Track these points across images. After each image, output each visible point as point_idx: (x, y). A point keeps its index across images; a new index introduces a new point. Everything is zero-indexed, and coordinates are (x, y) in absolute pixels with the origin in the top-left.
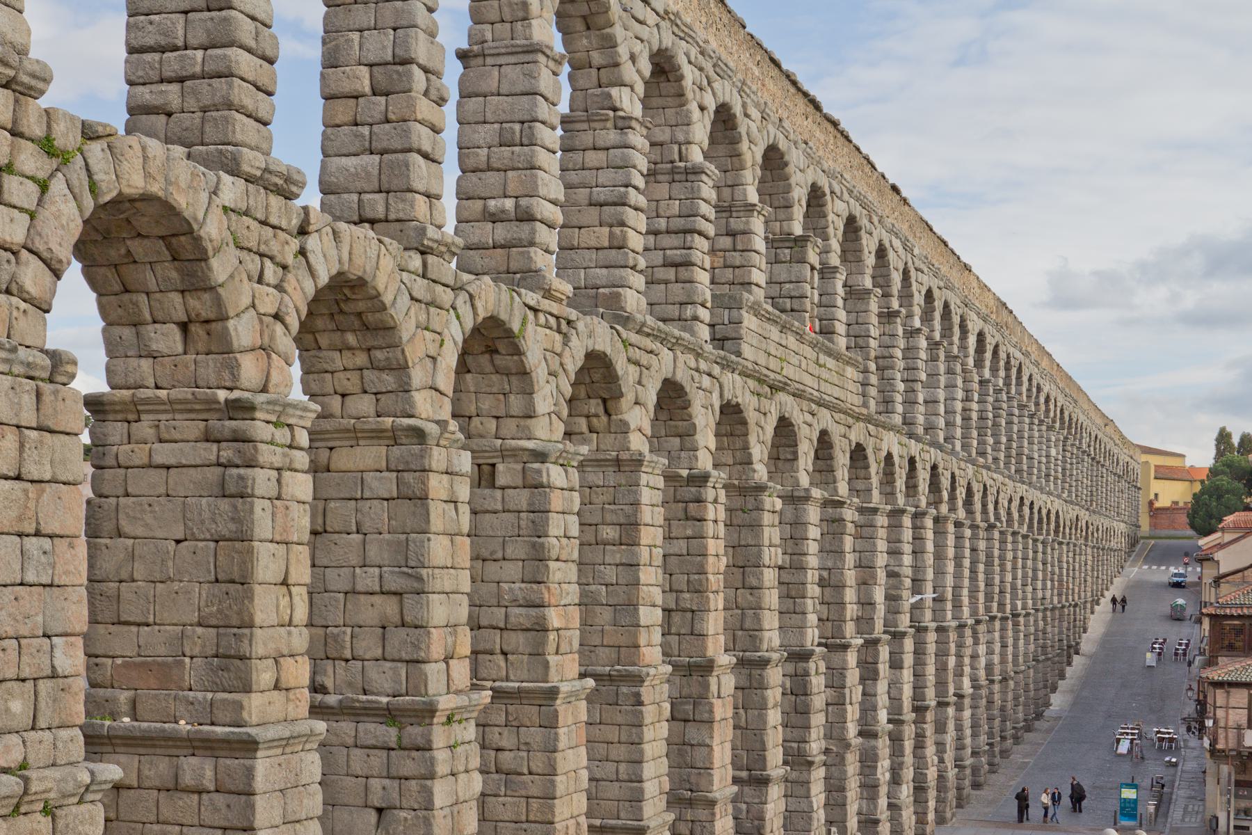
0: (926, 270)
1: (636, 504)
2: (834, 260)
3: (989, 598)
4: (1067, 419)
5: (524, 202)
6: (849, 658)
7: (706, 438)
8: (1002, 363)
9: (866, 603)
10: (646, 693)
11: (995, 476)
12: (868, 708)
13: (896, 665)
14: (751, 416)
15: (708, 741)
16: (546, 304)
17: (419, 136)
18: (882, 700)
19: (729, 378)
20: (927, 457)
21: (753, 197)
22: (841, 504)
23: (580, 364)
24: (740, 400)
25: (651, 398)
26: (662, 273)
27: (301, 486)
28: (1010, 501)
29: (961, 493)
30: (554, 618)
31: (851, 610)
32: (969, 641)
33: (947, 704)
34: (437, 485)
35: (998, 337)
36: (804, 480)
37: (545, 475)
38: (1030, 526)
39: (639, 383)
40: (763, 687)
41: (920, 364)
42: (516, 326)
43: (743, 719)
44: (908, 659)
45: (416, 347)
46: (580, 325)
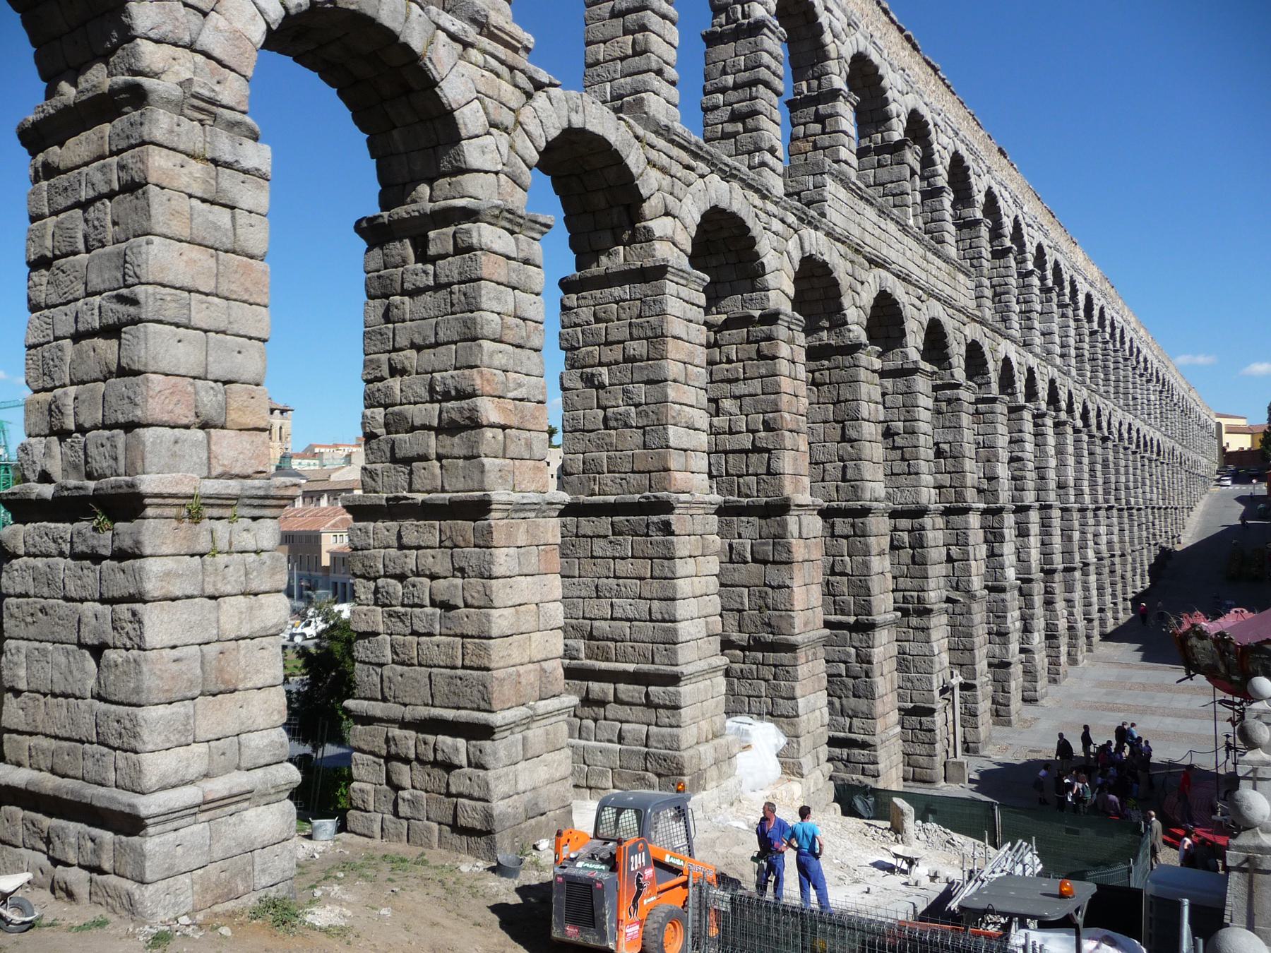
1: (663, 313)
2: (942, 181)
3: (1107, 492)
13: (1023, 533)
15: (788, 582)
16: (485, 42)
19: (807, 232)
20: (1045, 371)
22: (957, 386)
23: (554, 133)
24: (826, 258)
25: (692, 212)
26: (730, 128)
28: (1121, 424)
29: (1078, 409)
32: (1091, 521)
33: (1074, 569)
35: (1103, 302)
36: (914, 355)
37: (475, 234)
38: (1138, 446)
42: (417, 44)
44: (1034, 528)
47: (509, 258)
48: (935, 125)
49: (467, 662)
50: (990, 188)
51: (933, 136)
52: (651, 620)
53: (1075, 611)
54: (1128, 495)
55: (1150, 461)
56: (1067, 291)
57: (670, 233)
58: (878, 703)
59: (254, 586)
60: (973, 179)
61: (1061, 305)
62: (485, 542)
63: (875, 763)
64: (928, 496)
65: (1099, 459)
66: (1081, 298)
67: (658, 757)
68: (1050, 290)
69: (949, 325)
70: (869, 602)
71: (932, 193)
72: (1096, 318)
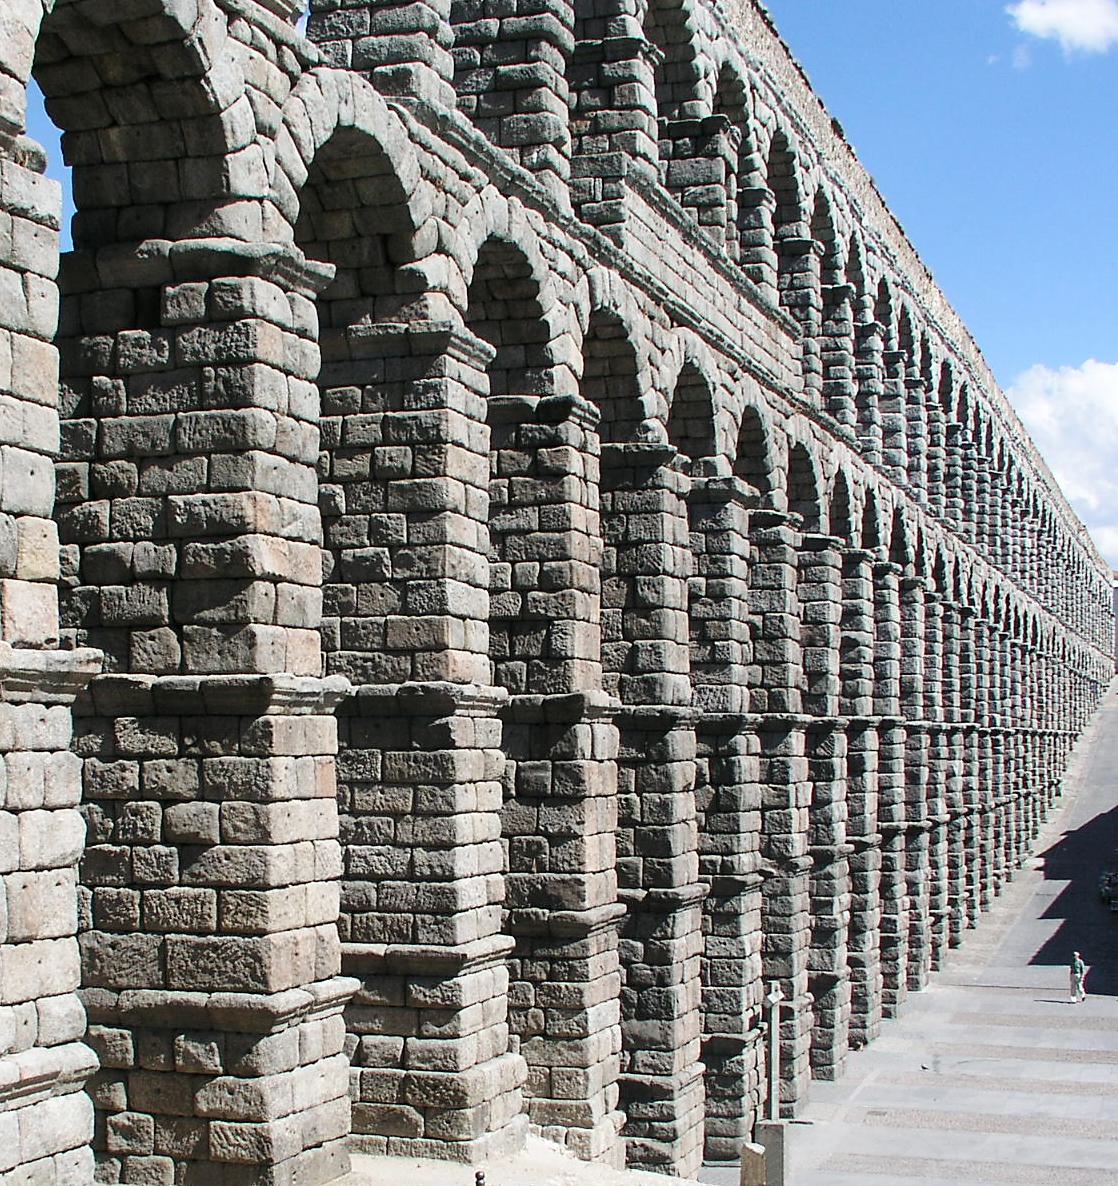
0: (878, 252)
1: (440, 404)
2: (759, 180)
4: (1040, 508)
6: (793, 741)
9: (815, 675)
10: (460, 725)
11: (968, 550)
15: (576, 828)
18: (839, 810)
19: (599, 271)
22: (778, 520)
24: (619, 312)
30: (265, 555)
31: (795, 673)
35: (965, 377)
36: (725, 470)
37: (246, 293)
38: (1007, 627)
43: (637, 810)
47: (284, 328)
48: (753, 87)
49: (228, 922)
50: (820, 187)
51: (749, 105)
52: (412, 880)
55: (1024, 649)
56: (917, 358)
57: (445, 282)
58: (677, 1023)
59: (53, 800)
60: (799, 172)
61: (911, 384)
63: (671, 1118)
64: (739, 699)
65: (957, 647)
66: (936, 369)
68: (896, 357)
69: (769, 418)
70: (669, 865)
71: (749, 201)
72: (954, 405)
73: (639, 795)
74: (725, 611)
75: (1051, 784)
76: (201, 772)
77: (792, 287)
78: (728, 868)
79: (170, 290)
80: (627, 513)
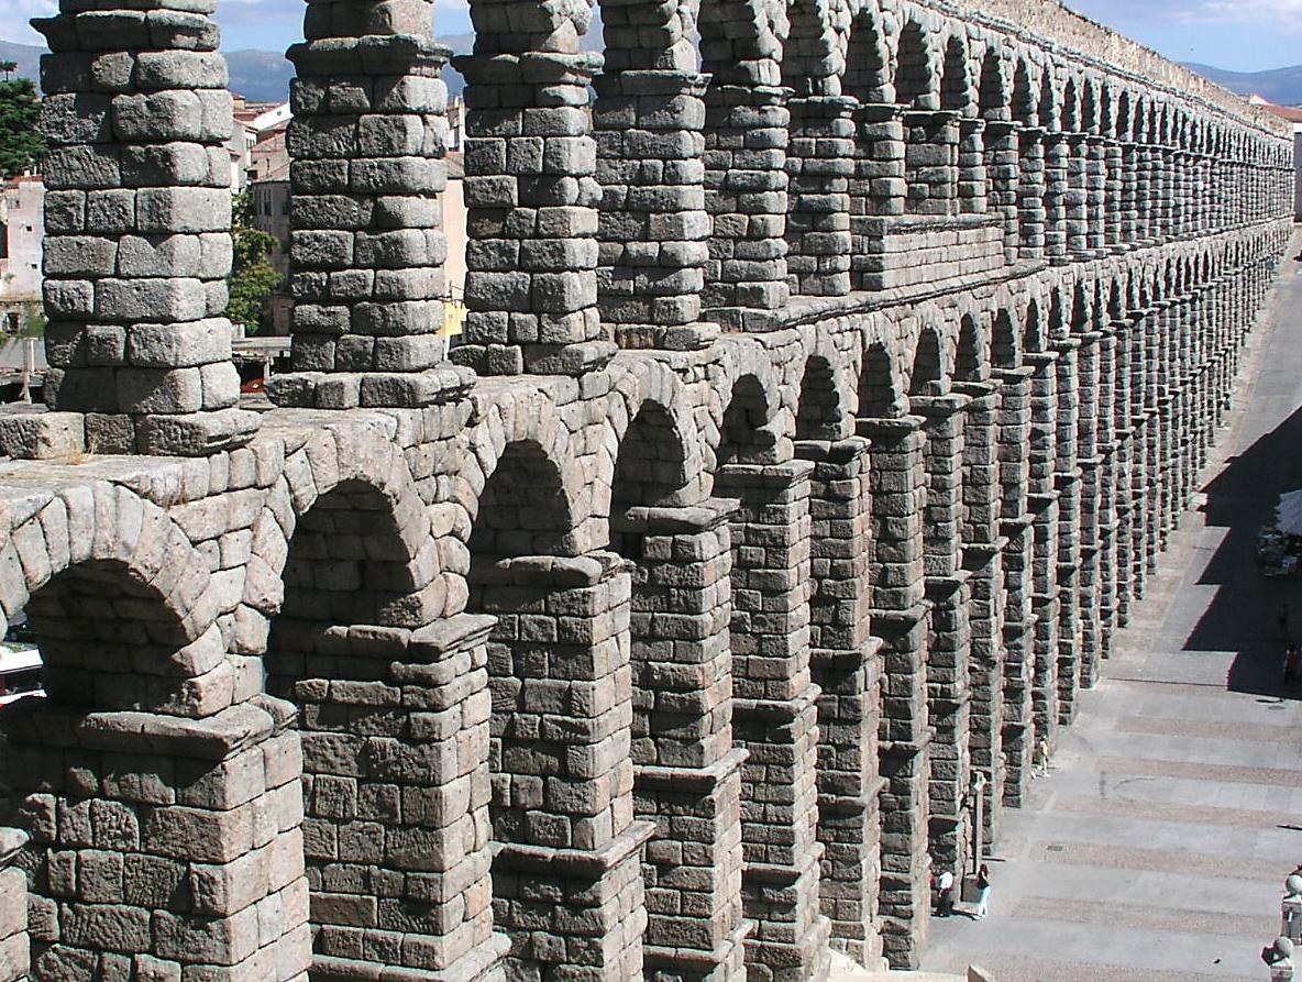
2: (973, 109)
4: (1214, 137)
5: (669, 246)
7: (849, 402)
8: (1146, 117)
12: (1014, 604)
14: (892, 350)
15: (854, 741)
17: (574, 254)
21: (889, 92)
25: (794, 392)
27: (482, 706)
30: (708, 700)
34: (599, 627)
36: (945, 383)
37: (697, 548)
39: (784, 382)
40: (906, 649)
41: (1062, 174)
45: (572, 485)
46: (727, 360)
48: (969, 38)
52: (765, 823)
53: (1090, 611)
54: (1162, 380)
62: (709, 811)
67: (773, 951)
73: (888, 674)
74: (945, 500)
75: (1219, 404)
76: (671, 824)
77: (995, 163)
78: (946, 694)
79: (648, 538)
80: (881, 471)
